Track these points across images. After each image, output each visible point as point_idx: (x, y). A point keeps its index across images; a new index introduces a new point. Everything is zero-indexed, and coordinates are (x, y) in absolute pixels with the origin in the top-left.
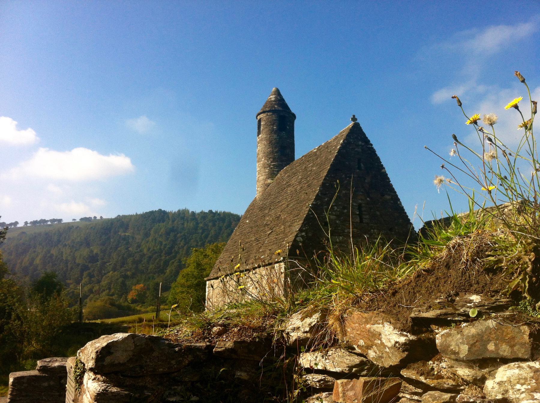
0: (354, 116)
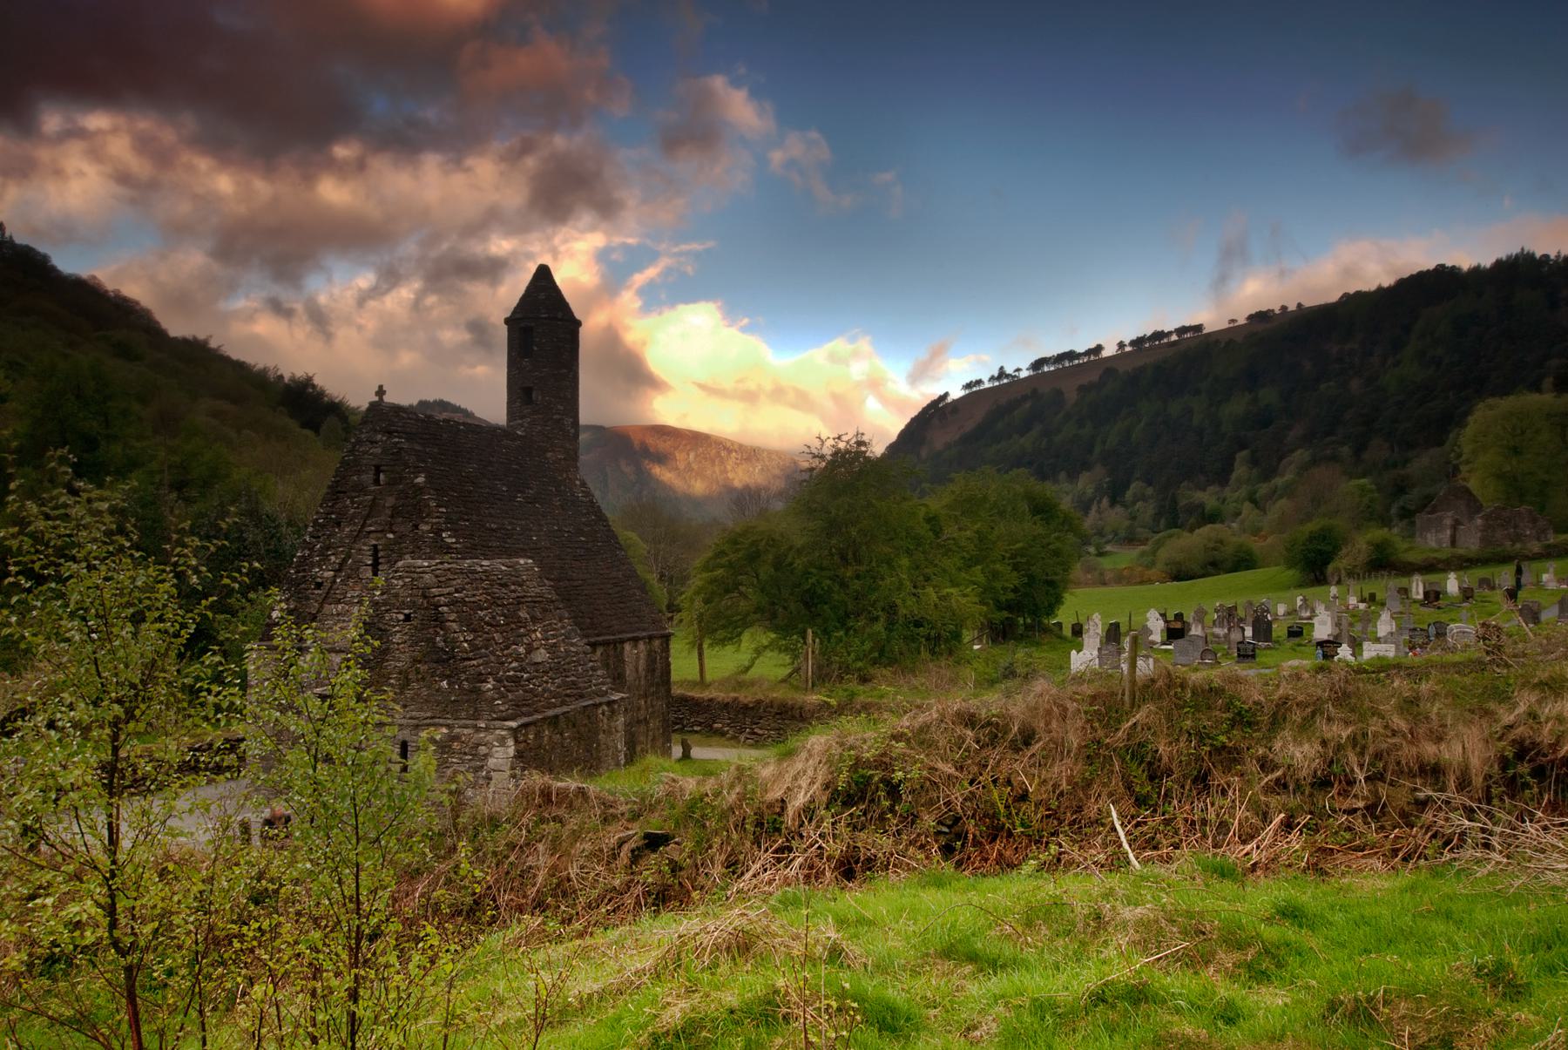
0: (381, 387)
